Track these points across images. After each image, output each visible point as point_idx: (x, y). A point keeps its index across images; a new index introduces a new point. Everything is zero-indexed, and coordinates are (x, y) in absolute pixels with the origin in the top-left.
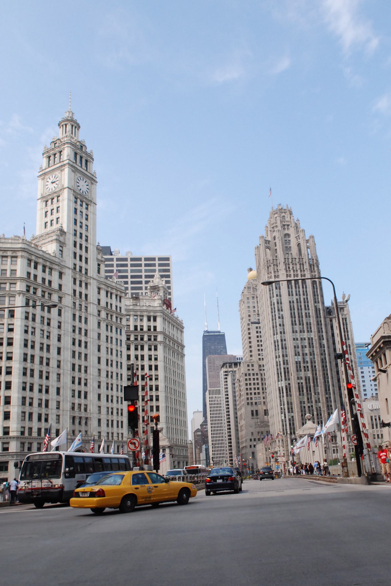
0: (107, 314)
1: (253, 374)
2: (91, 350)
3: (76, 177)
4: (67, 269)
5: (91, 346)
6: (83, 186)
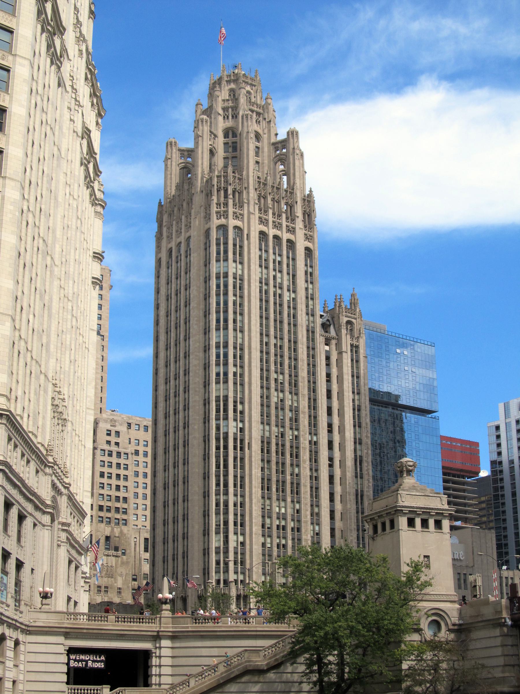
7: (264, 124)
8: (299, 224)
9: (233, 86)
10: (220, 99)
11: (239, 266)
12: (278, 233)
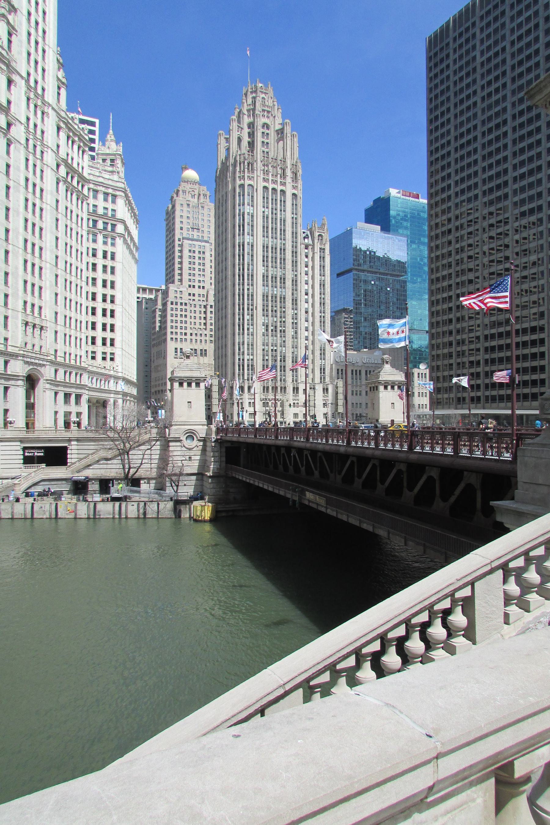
0: (68, 174)
1: (181, 304)
4: (18, 77)
7: (272, 118)
8: (289, 180)
9: (254, 95)
10: (245, 104)
11: (252, 208)
12: (275, 186)
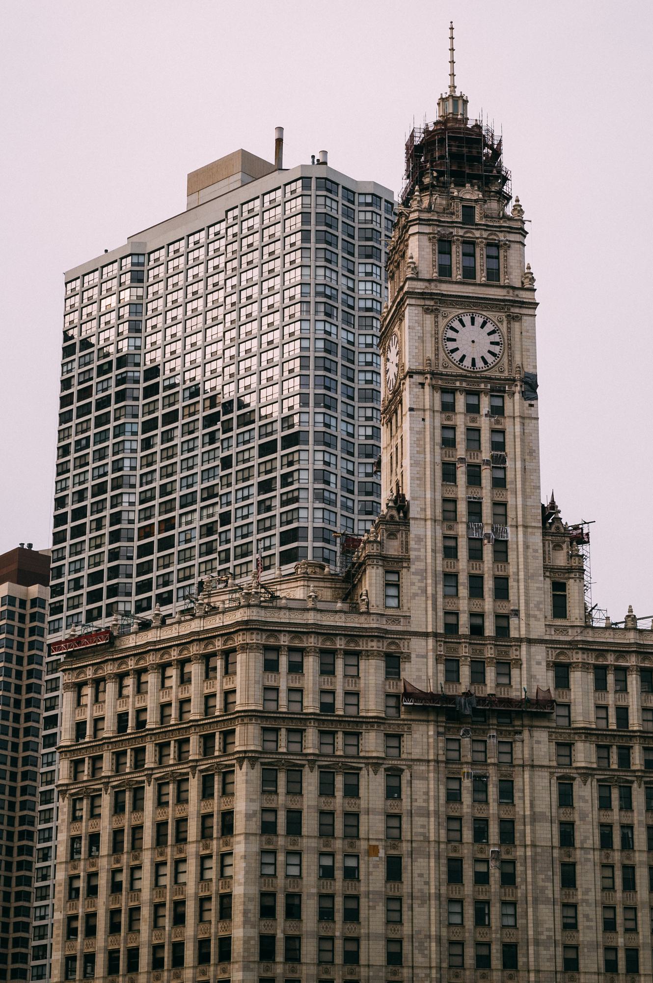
2: (530, 887)
3: (442, 323)
5: (529, 872)
6: (473, 341)
